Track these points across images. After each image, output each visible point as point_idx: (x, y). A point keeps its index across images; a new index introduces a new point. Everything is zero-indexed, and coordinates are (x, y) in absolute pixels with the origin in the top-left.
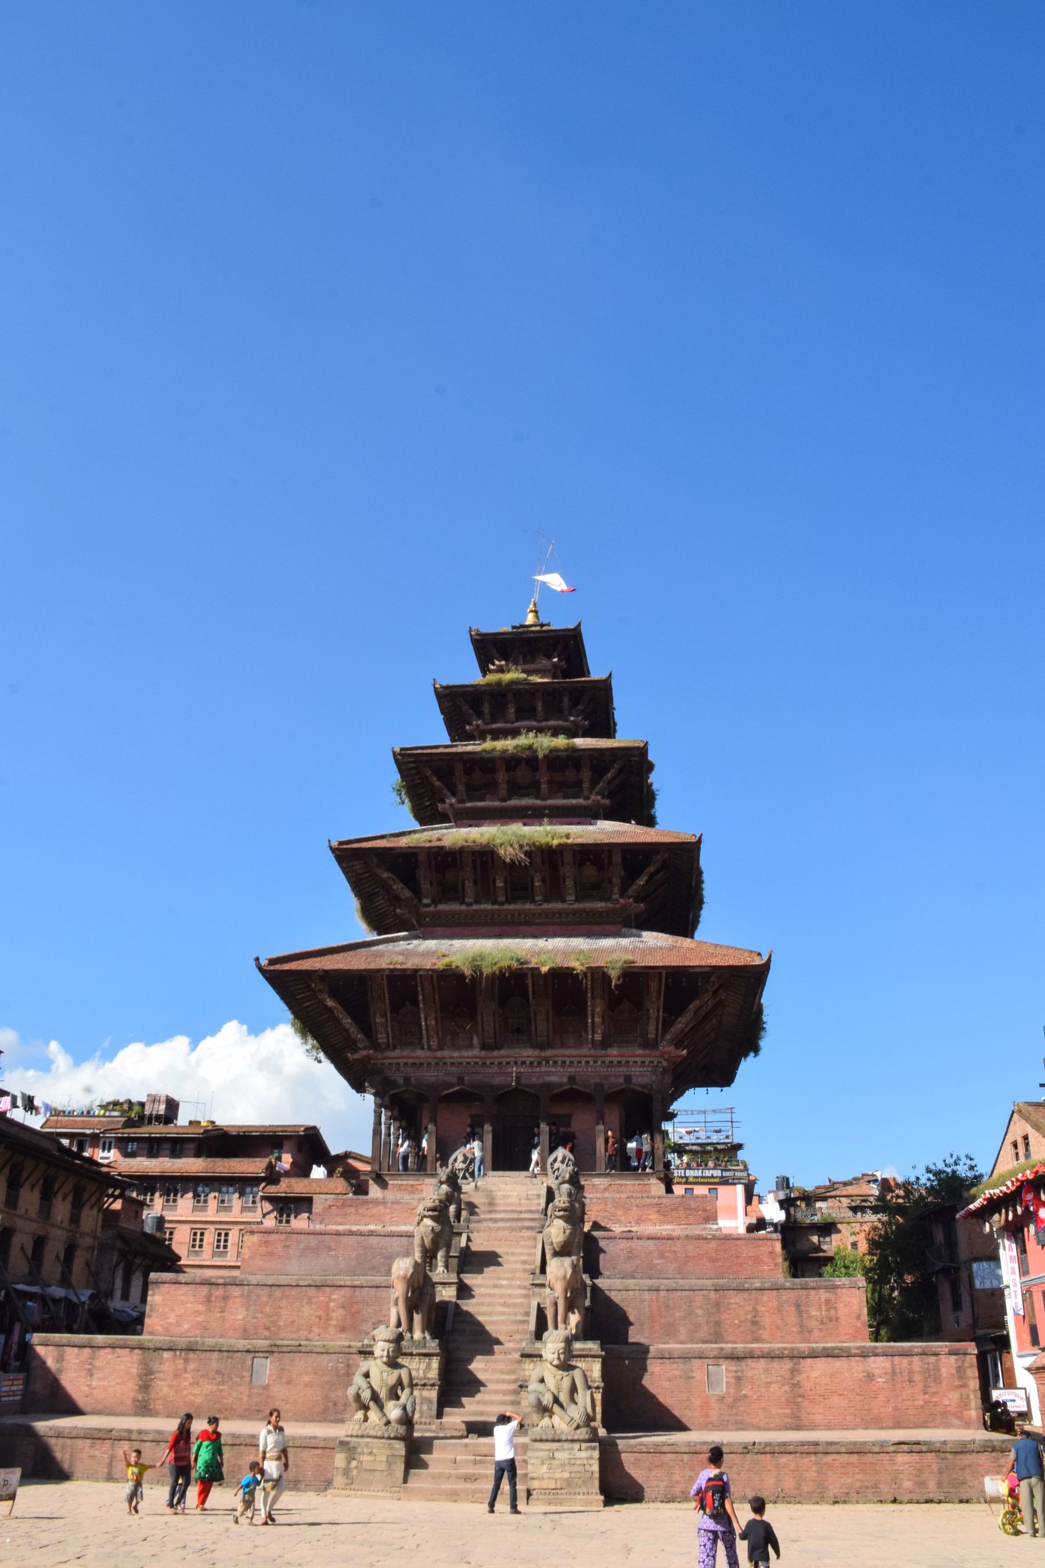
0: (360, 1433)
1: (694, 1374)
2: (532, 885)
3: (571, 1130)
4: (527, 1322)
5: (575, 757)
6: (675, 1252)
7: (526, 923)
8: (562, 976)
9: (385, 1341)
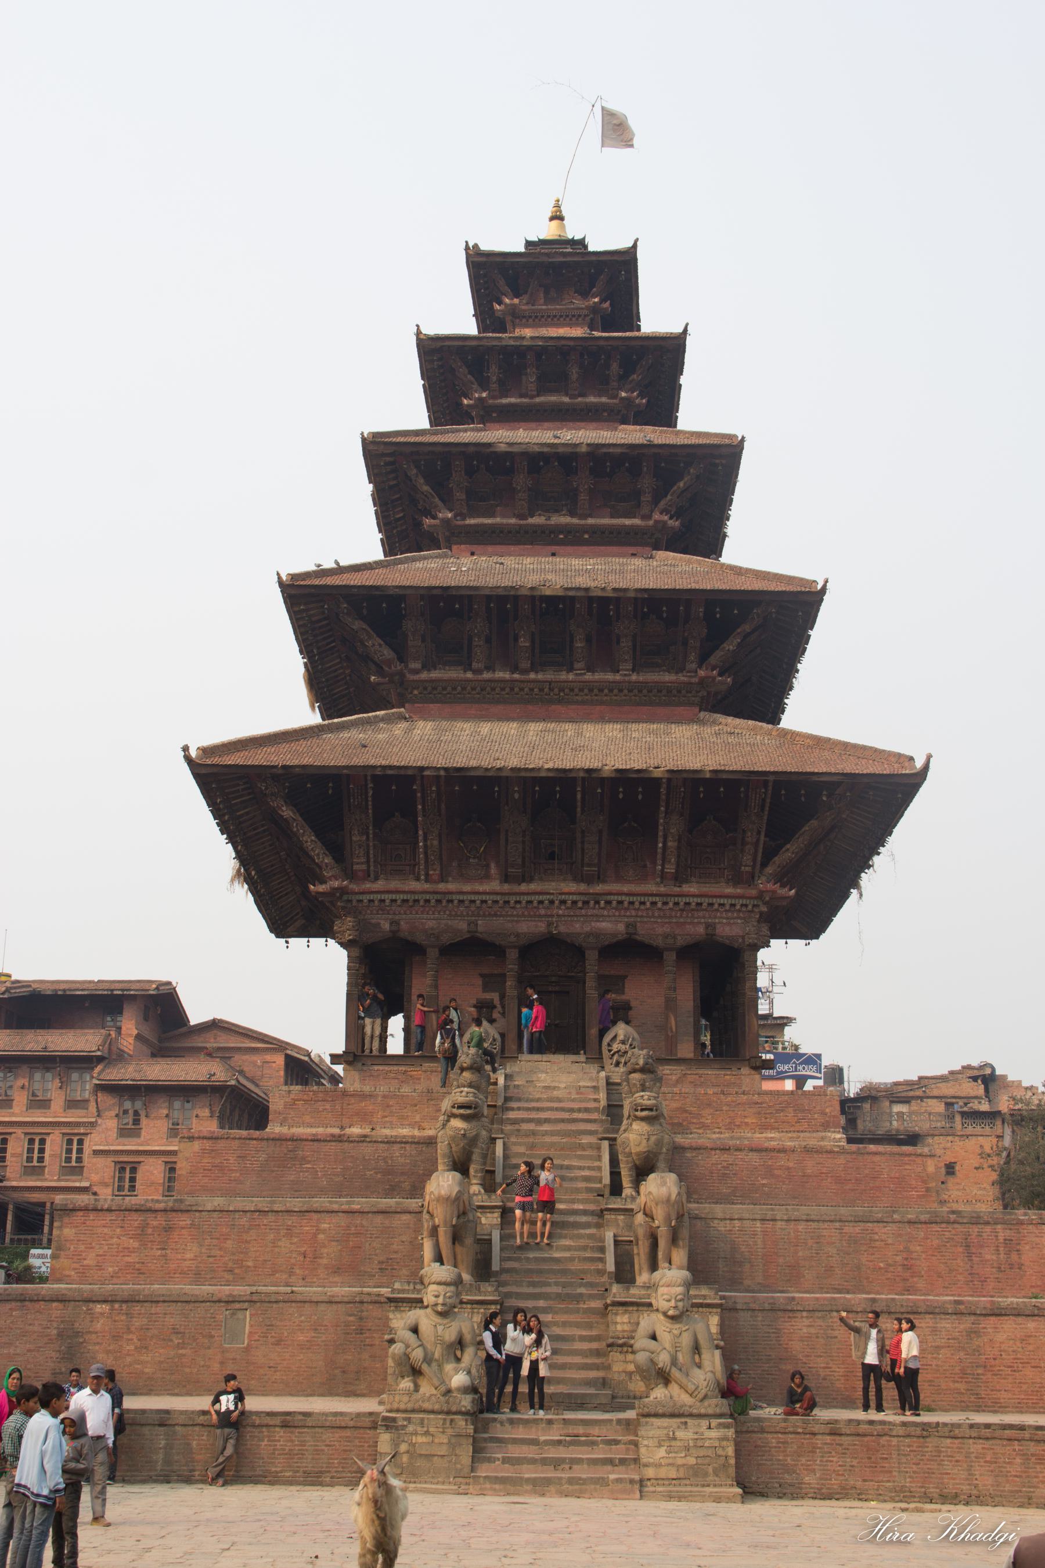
0: (410, 1406)
1: (836, 1333)
2: (572, 641)
3: (624, 997)
4: (602, 1260)
5: (632, 457)
6: (788, 1168)
7: (560, 701)
8: (631, 783)
9: (439, 1283)
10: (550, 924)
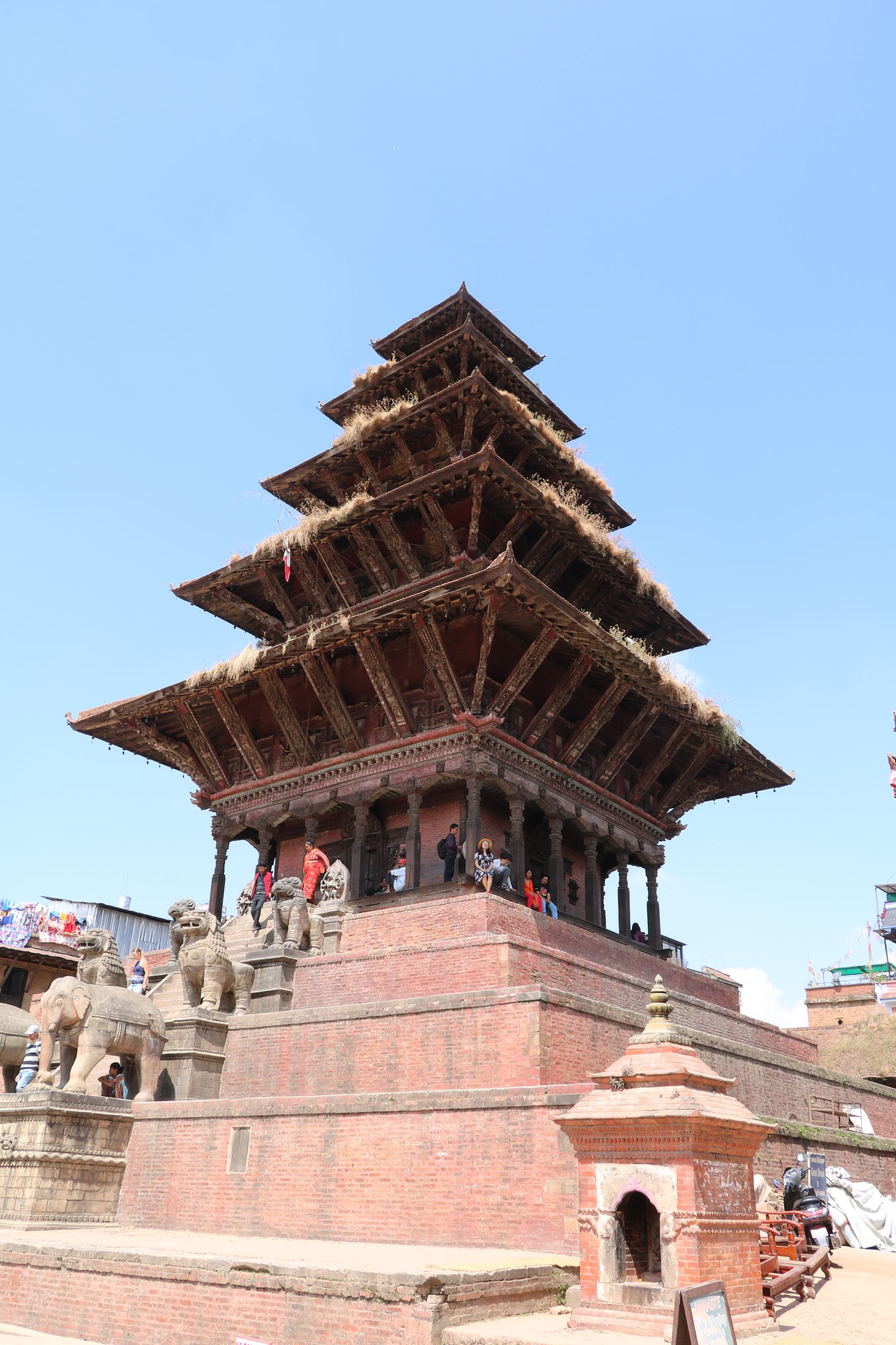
1: (217, 1143)
6: (385, 974)
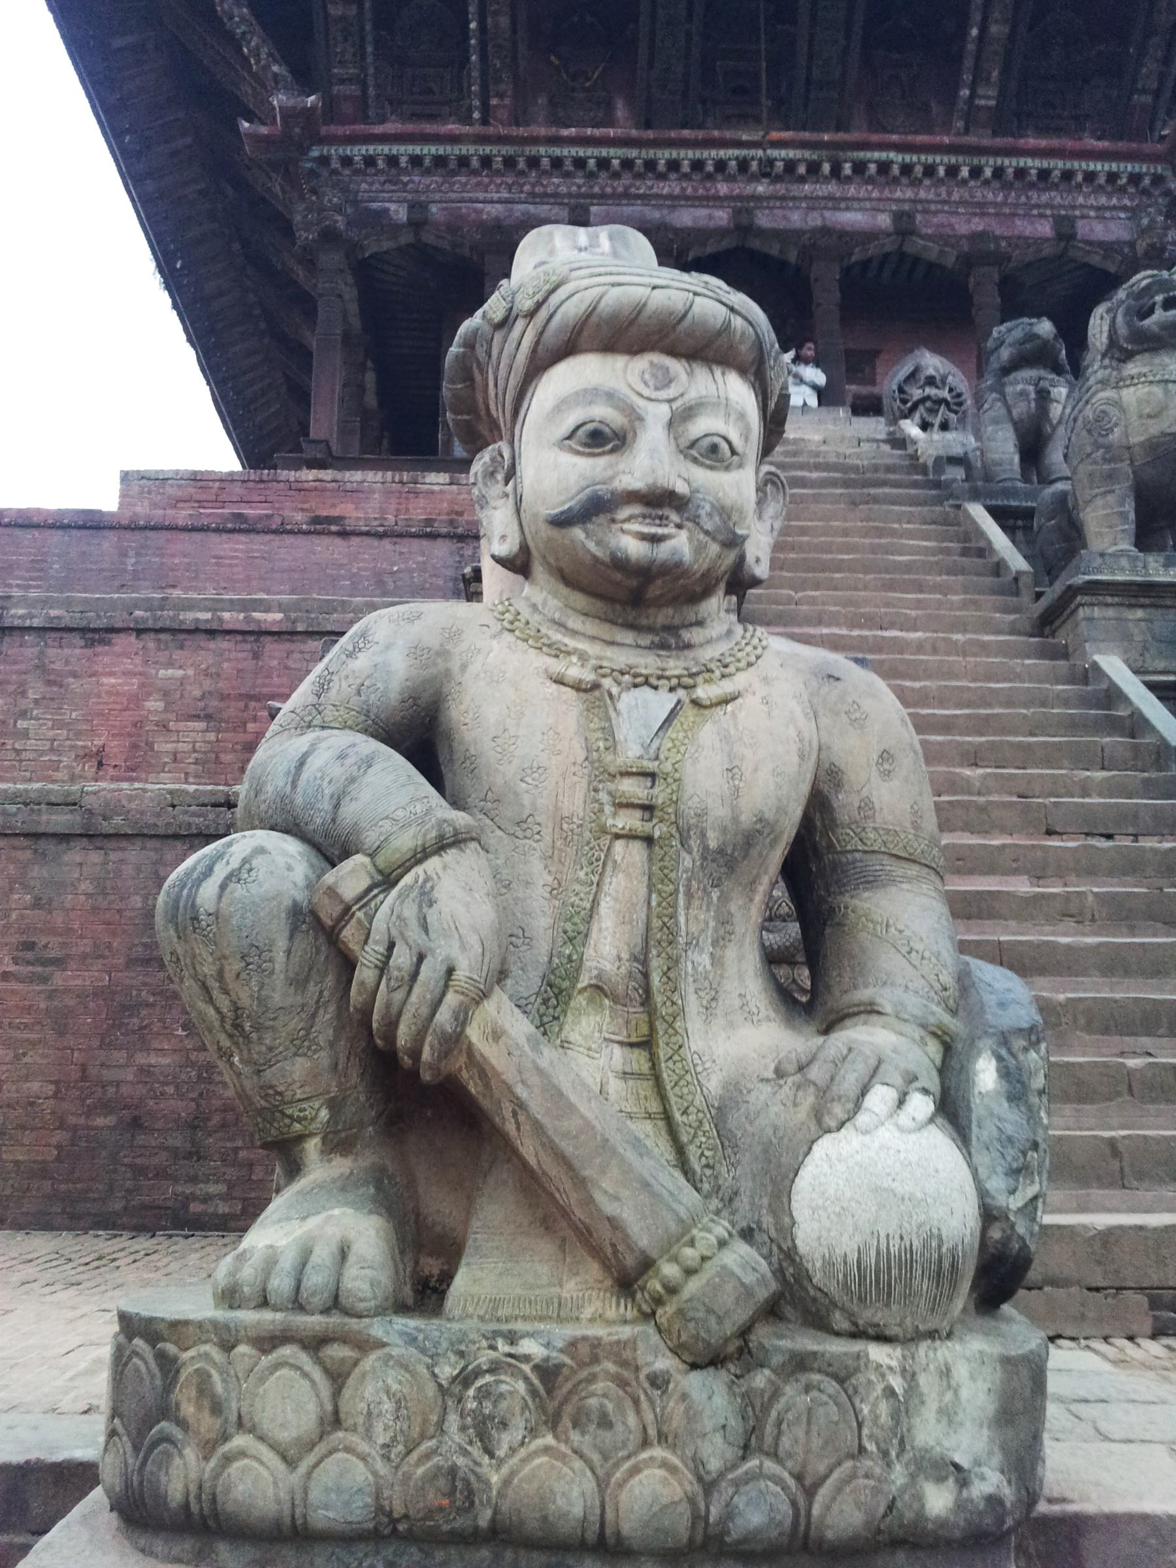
3: (876, 390)
10: (737, 212)
